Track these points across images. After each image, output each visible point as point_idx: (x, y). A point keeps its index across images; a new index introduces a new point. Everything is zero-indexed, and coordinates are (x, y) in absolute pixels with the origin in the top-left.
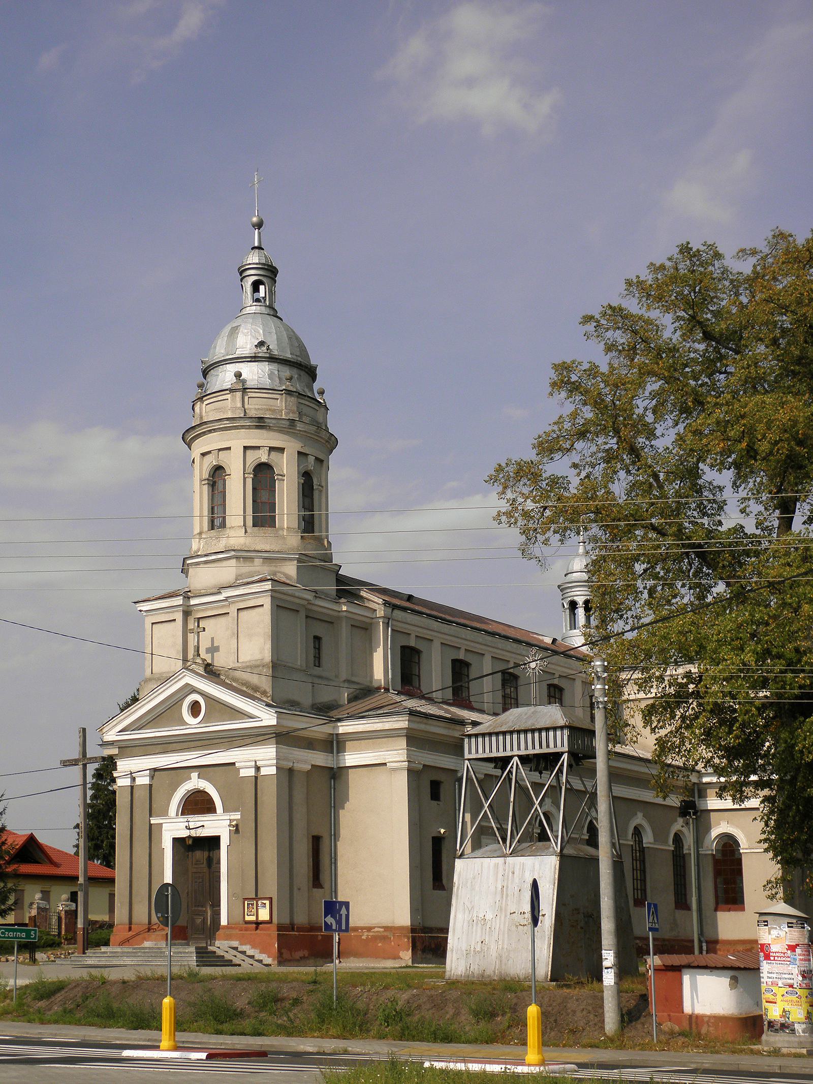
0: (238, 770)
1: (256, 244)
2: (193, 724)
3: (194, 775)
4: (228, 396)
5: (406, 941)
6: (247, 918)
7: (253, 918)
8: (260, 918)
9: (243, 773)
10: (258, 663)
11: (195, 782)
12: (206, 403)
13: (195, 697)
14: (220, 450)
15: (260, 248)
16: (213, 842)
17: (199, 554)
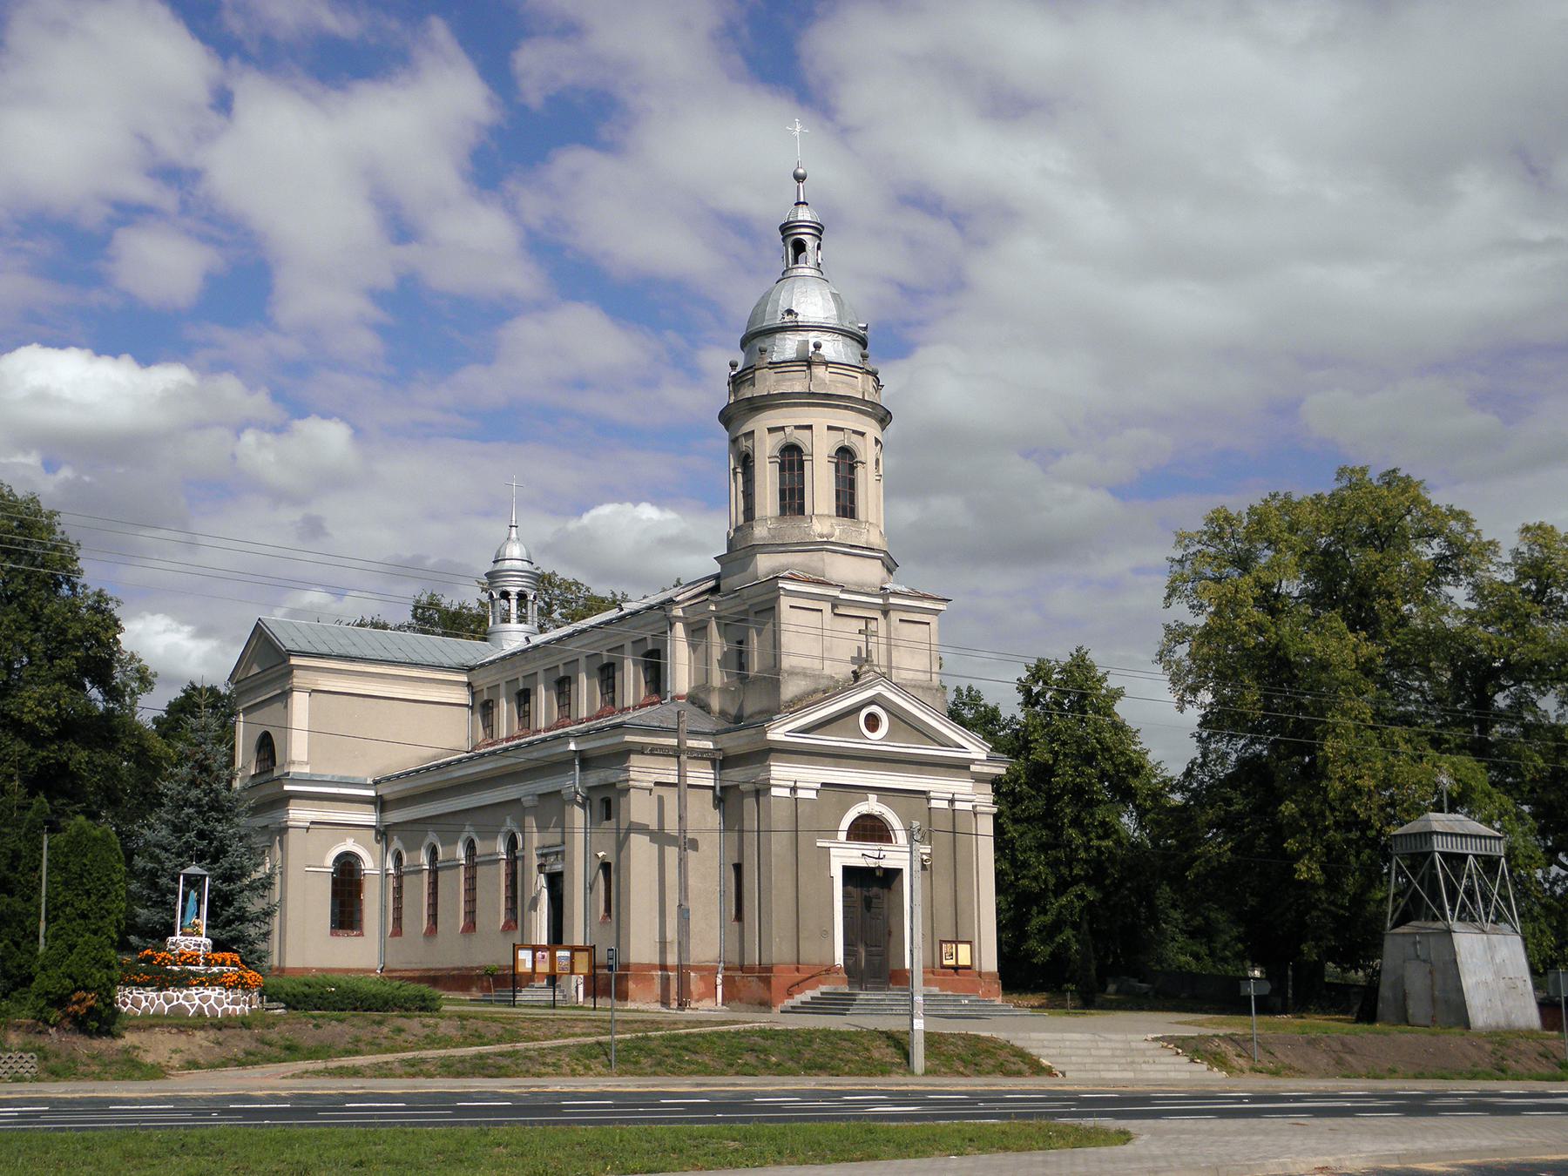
0: (929, 799)
1: (802, 200)
2: (876, 740)
3: (873, 797)
4: (859, 375)
5: (997, 986)
6: (946, 962)
7: (952, 962)
8: (960, 963)
9: (934, 804)
10: (926, 684)
11: (872, 806)
12: (829, 369)
13: (874, 709)
14: (855, 432)
15: (804, 203)
16: (893, 875)
17: (833, 539)
